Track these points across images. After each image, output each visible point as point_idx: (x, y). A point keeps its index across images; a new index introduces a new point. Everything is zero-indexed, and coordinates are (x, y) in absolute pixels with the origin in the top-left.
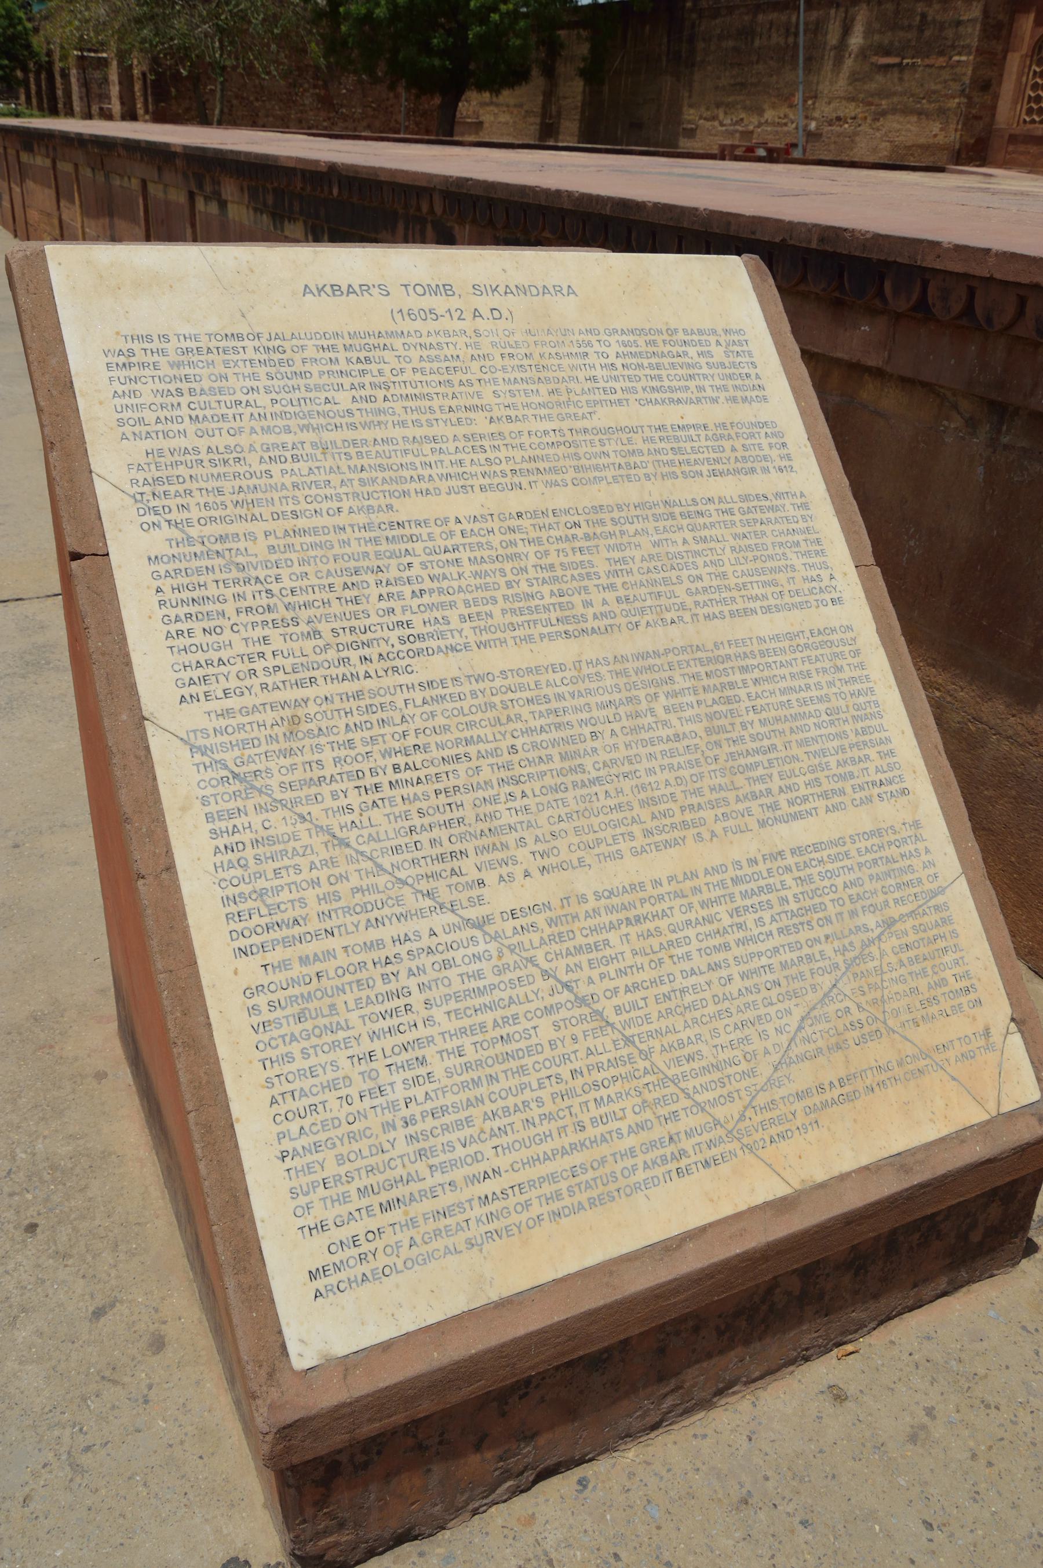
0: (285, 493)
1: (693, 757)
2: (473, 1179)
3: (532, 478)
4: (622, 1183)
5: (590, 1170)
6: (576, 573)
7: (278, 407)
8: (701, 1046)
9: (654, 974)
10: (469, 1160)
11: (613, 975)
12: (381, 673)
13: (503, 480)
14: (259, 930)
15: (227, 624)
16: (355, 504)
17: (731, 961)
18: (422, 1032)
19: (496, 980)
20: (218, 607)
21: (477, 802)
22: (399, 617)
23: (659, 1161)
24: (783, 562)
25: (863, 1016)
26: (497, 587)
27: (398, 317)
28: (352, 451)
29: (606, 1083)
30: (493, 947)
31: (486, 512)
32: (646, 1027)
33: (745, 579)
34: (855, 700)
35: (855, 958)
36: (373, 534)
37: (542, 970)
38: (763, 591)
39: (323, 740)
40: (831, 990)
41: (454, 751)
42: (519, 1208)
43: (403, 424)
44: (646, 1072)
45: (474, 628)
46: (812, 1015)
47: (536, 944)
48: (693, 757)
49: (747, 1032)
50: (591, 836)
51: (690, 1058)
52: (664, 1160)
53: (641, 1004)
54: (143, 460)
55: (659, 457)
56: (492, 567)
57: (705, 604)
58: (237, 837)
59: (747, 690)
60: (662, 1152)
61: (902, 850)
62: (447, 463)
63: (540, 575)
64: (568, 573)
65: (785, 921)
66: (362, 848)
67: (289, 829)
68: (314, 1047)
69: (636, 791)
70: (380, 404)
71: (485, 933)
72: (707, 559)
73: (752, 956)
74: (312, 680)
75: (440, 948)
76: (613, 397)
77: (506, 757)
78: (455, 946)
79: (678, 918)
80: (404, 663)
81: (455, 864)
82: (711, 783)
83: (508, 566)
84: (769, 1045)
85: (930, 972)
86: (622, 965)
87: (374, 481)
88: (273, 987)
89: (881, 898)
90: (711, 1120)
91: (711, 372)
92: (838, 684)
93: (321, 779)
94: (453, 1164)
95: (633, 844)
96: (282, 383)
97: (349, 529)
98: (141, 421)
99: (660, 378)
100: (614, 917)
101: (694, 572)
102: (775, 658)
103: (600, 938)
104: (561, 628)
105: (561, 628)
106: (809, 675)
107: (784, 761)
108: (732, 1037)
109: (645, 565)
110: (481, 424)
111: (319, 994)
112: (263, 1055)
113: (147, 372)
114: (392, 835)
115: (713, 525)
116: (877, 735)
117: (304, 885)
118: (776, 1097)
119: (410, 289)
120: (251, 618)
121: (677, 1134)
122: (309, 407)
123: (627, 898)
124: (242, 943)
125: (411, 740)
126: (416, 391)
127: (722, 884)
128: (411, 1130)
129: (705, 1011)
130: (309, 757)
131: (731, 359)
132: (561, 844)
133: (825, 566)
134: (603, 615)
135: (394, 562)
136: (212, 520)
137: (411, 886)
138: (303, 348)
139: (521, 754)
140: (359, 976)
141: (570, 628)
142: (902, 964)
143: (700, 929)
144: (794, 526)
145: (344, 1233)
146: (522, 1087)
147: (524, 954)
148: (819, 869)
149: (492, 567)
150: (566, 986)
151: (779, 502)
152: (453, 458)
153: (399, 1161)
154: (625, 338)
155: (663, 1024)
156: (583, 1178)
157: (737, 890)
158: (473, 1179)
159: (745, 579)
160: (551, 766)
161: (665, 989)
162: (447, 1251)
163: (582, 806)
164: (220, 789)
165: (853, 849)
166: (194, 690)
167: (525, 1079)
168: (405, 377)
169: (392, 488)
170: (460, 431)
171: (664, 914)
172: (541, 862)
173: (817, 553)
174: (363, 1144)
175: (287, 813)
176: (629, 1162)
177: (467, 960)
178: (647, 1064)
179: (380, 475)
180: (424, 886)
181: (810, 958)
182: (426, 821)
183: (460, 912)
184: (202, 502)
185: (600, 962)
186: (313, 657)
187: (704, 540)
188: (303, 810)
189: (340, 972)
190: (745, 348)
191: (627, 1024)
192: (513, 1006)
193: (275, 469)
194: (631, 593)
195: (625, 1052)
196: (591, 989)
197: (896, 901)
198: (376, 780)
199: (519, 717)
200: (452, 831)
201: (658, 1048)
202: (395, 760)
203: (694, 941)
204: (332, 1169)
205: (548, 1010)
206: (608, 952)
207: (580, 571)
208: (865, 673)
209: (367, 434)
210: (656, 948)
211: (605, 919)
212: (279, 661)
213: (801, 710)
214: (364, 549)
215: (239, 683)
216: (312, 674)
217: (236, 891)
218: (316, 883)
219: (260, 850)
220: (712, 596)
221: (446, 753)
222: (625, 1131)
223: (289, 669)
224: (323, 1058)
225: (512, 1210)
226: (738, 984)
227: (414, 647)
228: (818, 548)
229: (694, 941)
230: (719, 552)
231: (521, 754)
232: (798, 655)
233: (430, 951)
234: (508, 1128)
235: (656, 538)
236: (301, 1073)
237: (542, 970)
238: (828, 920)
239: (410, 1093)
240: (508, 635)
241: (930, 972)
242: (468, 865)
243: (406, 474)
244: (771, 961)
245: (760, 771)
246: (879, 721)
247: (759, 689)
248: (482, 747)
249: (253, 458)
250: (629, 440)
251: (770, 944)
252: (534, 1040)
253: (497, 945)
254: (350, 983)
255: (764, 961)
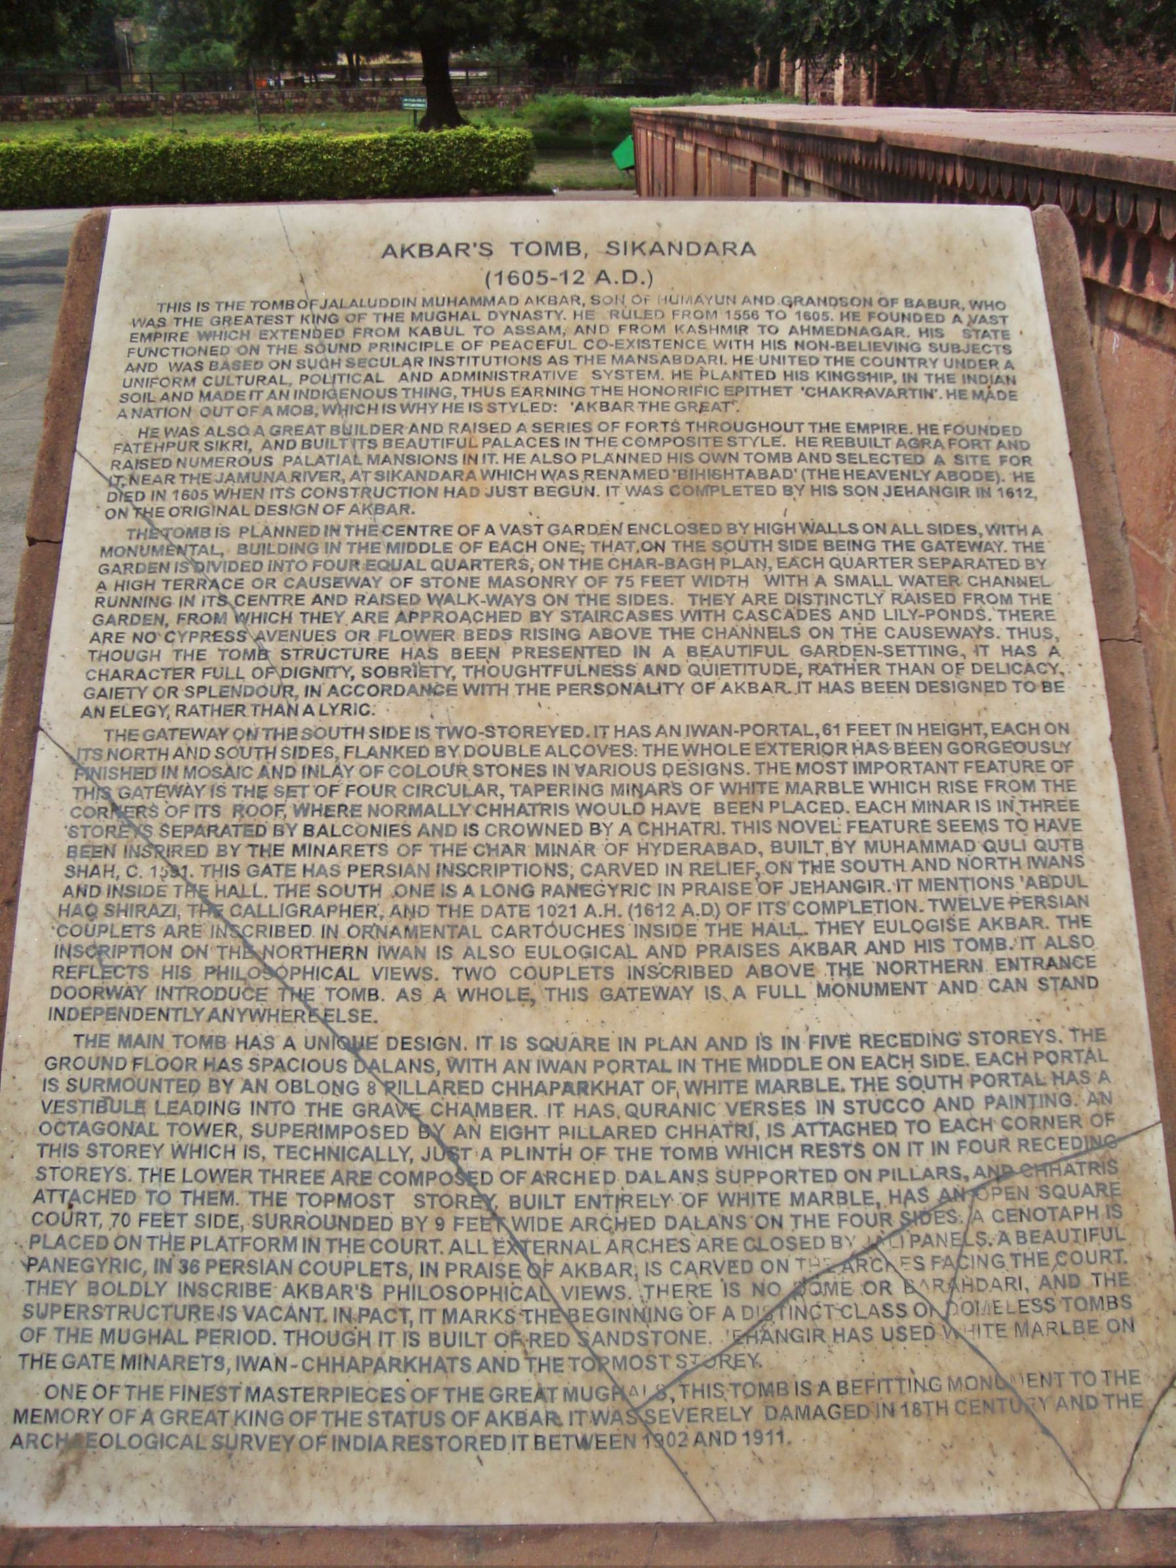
0: (281, 484)
1: (738, 879)
2: (247, 1363)
3: (613, 482)
4: (449, 1430)
5: (408, 1401)
6: (637, 610)
7: (307, 384)
8: (626, 1281)
9: (587, 1167)
10: (250, 1338)
11: (522, 1153)
12: (327, 709)
13: (569, 483)
14: (85, 993)
15: (163, 631)
16: (358, 501)
17: (712, 1177)
18: (238, 1162)
19: (354, 1122)
20: (160, 611)
21: (401, 890)
22: (373, 643)
23: (512, 1417)
24: (975, 623)
25: (911, 1300)
26: (516, 616)
27: (494, 280)
28: (380, 438)
29: (467, 1293)
30: (363, 1079)
31: (532, 521)
32: (550, 1235)
33: (903, 641)
34: (1041, 834)
35: (924, 1213)
36: (372, 539)
37: (422, 1125)
38: (928, 660)
39: (229, 782)
40: (867, 1250)
41: (392, 820)
42: (297, 1419)
43: (457, 408)
44: (531, 1294)
45: (468, 668)
46: (824, 1278)
47: (424, 1087)
48: (738, 879)
49: (704, 1278)
50: (551, 963)
51: (602, 1293)
52: (521, 1419)
53: (552, 1202)
54: (133, 439)
55: (814, 465)
56: (519, 591)
57: (827, 669)
58: (94, 880)
59: (859, 797)
60: (520, 1406)
61: (1057, 1069)
62: (499, 458)
63: (585, 608)
64: (626, 609)
65: (818, 1137)
66: (235, 921)
67: (156, 882)
68: (105, 1146)
69: (635, 912)
70: (436, 383)
71: (359, 1059)
72: (849, 608)
73: (748, 1174)
74: (239, 709)
75: (294, 1065)
76: (768, 384)
77: (460, 838)
78: (314, 1066)
79: (646, 1097)
80: (360, 701)
81: (346, 963)
82: (758, 920)
83: (539, 593)
84: (736, 1304)
85: (1052, 1261)
86: (539, 1144)
87: (395, 475)
88: (79, 1063)
89: (998, 1133)
90: (610, 1385)
91: (934, 356)
92: (1018, 807)
93: (212, 829)
94: (228, 1336)
95: (609, 984)
96: (320, 357)
97: (344, 531)
98: (147, 397)
99: (849, 361)
100: (548, 1078)
101: (821, 624)
102: (918, 758)
103: (519, 1100)
104: (593, 679)
105: (593, 679)
106: (972, 787)
107: (889, 907)
108: (679, 1280)
109: (748, 607)
110: (564, 411)
111: (129, 1085)
112: (45, 1139)
113: (173, 343)
114: (276, 910)
115: (873, 561)
116: (1064, 892)
117: (153, 951)
118: (725, 1381)
119: (522, 251)
120: (192, 627)
121: (552, 1390)
122: (345, 384)
123: (575, 1055)
124: (61, 1003)
125: (338, 798)
126: (488, 369)
127: (732, 1065)
128: (189, 1278)
129: (648, 1235)
130: (206, 799)
131: (973, 340)
132: (502, 965)
133: (1047, 634)
134: (661, 669)
135: (386, 575)
136: (186, 510)
137: (281, 979)
138: (360, 317)
139: (482, 838)
140: (182, 1074)
141: (605, 681)
142: (1004, 1238)
143: (675, 1120)
144: (1009, 573)
145: (71, 1378)
146: (346, 1267)
147: (404, 1098)
148: (901, 1072)
149: (519, 591)
150: (450, 1153)
151: (994, 538)
152: (509, 451)
153: (162, 1312)
154: (811, 309)
155: (575, 1236)
156: (396, 1408)
157: (752, 1077)
158: (247, 1363)
159: (903, 641)
160: (520, 859)
161: (597, 1190)
162: (187, 1442)
163: (547, 920)
164: (94, 821)
165: (969, 1053)
166: (101, 702)
167: (355, 1258)
168: (480, 351)
169: (414, 485)
170: (529, 419)
171: (626, 1087)
172: (464, 983)
173: (1037, 615)
174: (125, 1279)
175: (160, 863)
176: (468, 1407)
177: (323, 1087)
178: (536, 1285)
179: (406, 468)
180: (297, 983)
181: (844, 1197)
182: (326, 902)
183: (334, 1025)
184: (181, 489)
185: (507, 1133)
186: (250, 681)
187: (854, 581)
188: (177, 861)
189: (162, 1064)
190: (1000, 327)
191: (521, 1224)
192: (367, 1161)
193: (278, 455)
194: (712, 644)
195: (507, 1260)
196: (486, 1165)
197: (1023, 1143)
198: (278, 840)
199: (493, 789)
200: (356, 921)
201: (558, 1268)
202: (309, 820)
203: (661, 1134)
204: (80, 1295)
205: (415, 1178)
206: (522, 1122)
207: (645, 607)
208: (1071, 796)
209: (406, 419)
210: (598, 1131)
211: (535, 1077)
212: (209, 681)
213: (942, 838)
214: (355, 556)
215: (154, 702)
216: (242, 700)
217: (75, 941)
218: (167, 951)
219: (115, 900)
220: (843, 660)
221: (379, 821)
222: (475, 1364)
223: (215, 692)
224: (109, 1162)
225: (286, 1417)
226: (713, 1206)
227: (379, 682)
228: (1043, 608)
229: (661, 1134)
230: (872, 599)
231: (482, 838)
232: (961, 757)
233: (280, 1065)
234: (314, 1313)
235: (776, 572)
236: (80, 1173)
237: (422, 1125)
238: (895, 1150)
239: (202, 1233)
240: (515, 679)
241: (1052, 1261)
242: (363, 970)
243: (440, 468)
244: (776, 1189)
245: (846, 915)
246: (1075, 870)
247: (879, 798)
248: (429, 821)
249: (256, 443)
250: (774, 441)
251: (782, 1165)
252: (382, 1212)
253: (370, 1078)
254: (169, 1081)
255: (766, 1186)
